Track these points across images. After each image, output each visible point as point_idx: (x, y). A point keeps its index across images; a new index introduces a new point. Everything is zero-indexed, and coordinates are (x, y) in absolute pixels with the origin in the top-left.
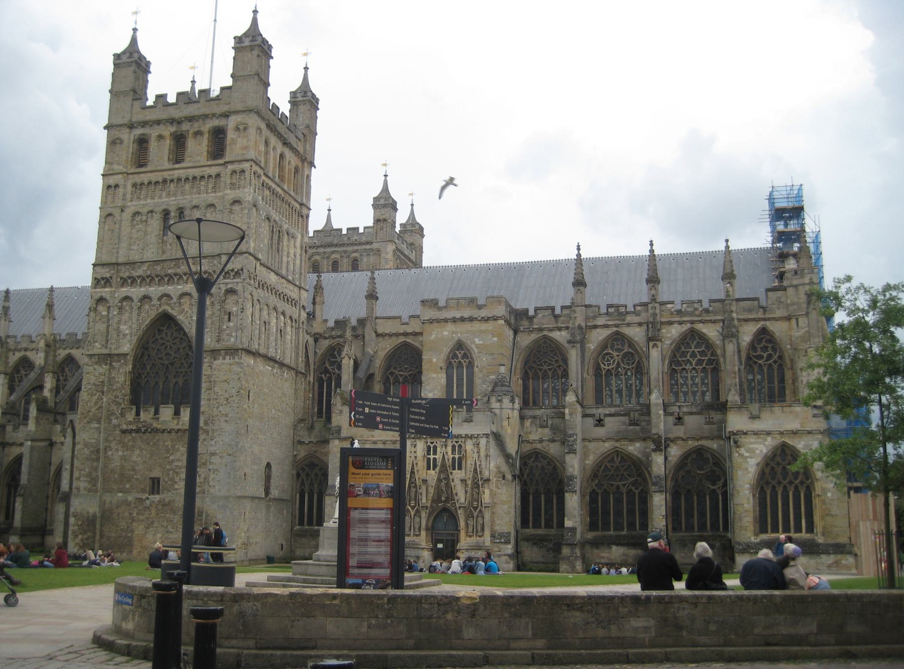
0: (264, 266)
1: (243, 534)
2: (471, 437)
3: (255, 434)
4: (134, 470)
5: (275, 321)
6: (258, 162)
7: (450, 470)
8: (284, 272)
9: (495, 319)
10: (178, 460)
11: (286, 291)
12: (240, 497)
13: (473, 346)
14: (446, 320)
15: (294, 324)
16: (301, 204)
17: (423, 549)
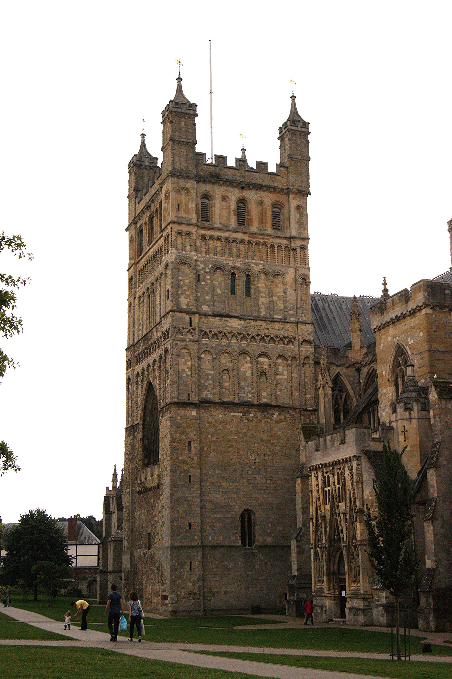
0: (215, 316)
1: (190, 584)
2: (347, 461)
3: (213, 483)
4: (142, 528)
5: (249, 365)
7: (336, 504)
8: (263, 313)
9: (419, 309)
10: (155, 516)
11: (263, 332)
12: (180, 547)
13: (407, 348)
14: (387, 324)
15: (289, 362)
16: (290, 238)
17: (326, 597)
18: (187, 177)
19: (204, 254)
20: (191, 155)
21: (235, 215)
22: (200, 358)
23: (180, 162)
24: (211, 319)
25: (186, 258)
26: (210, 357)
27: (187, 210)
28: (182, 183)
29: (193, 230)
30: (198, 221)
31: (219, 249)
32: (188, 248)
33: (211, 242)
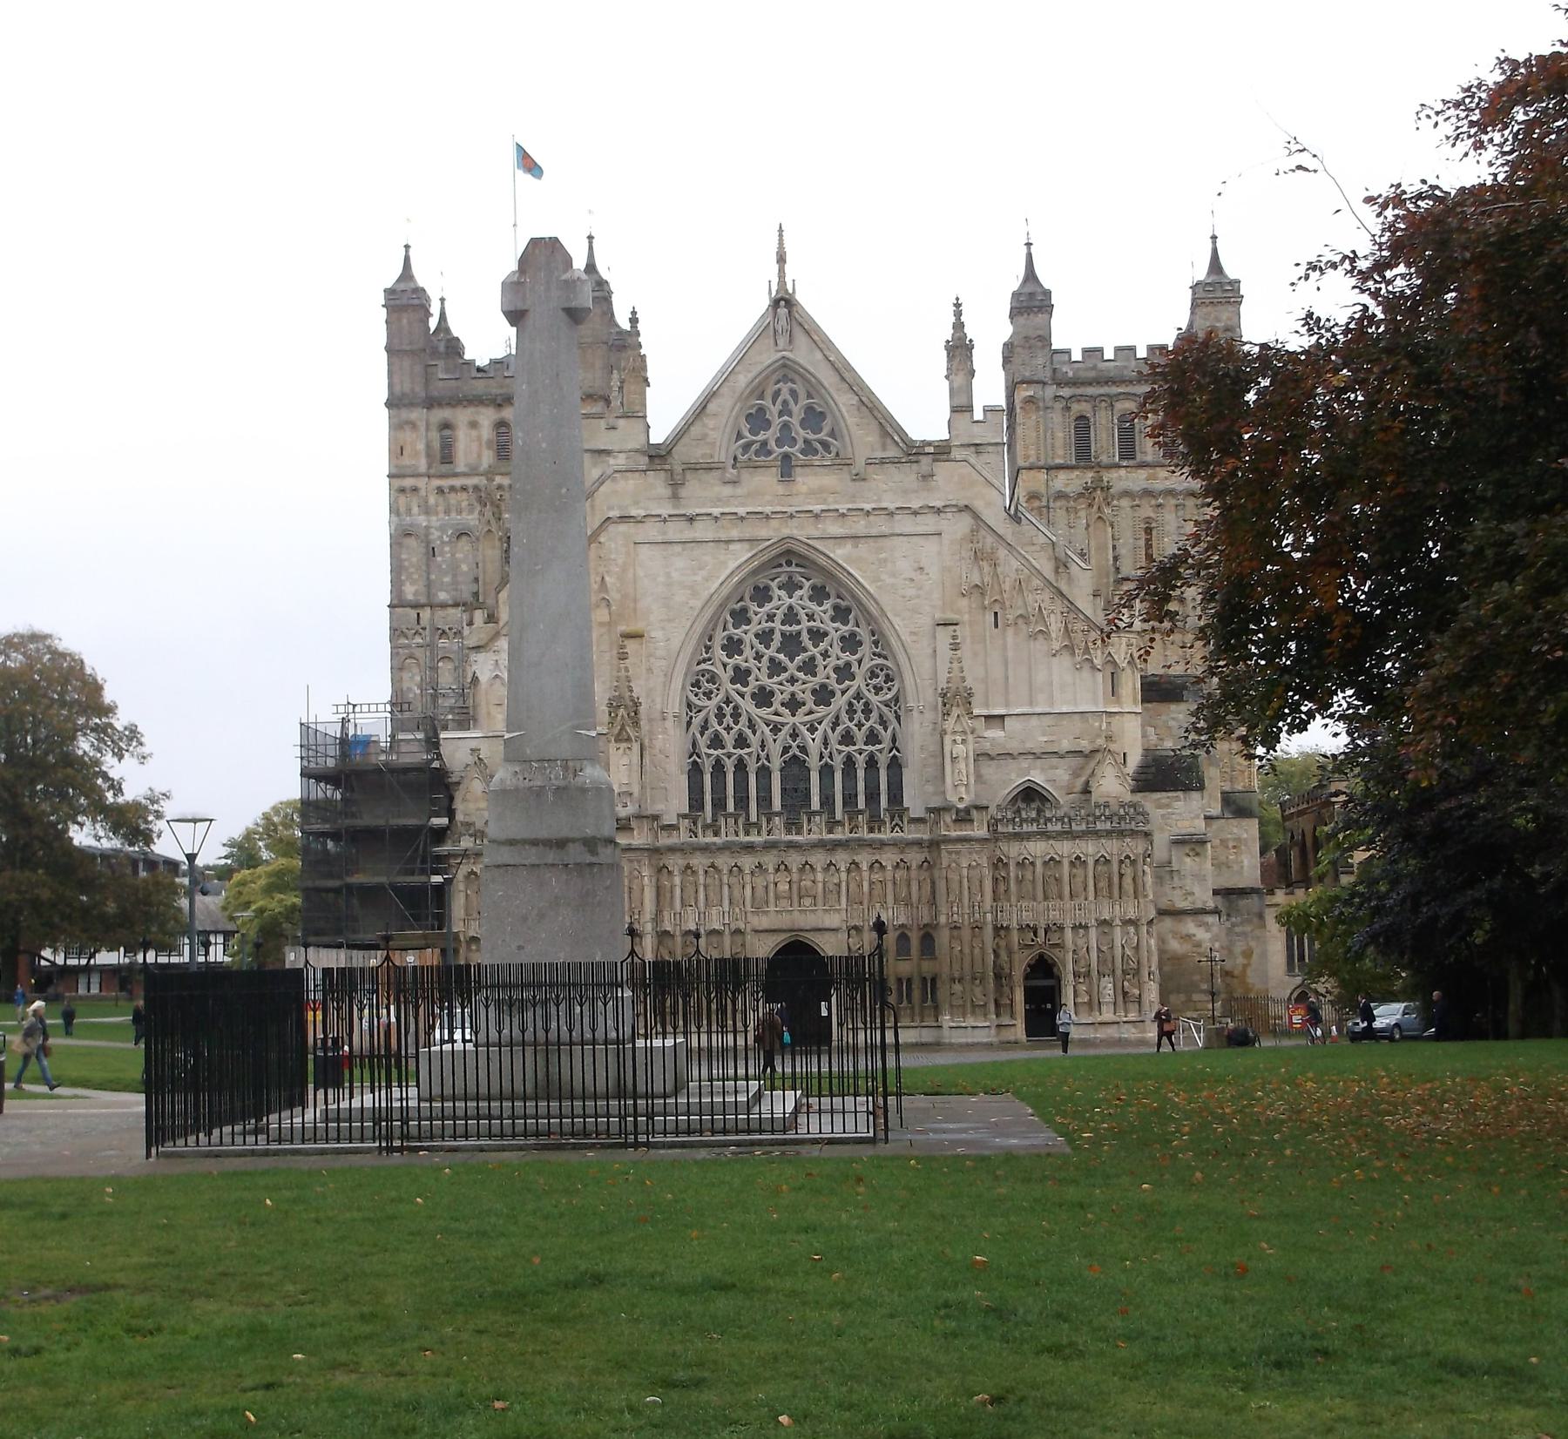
6: (408, 471)
18: (412, 405)
19: (441, 515)
20: (418, 369)
21: (489, 448)
22: (435, 669)
23: (402, 382)
24: (451, 611)
25: (411, 525)
26: (450, 666)
27: (416, 454)
28: (405, 414)
29: (421, 483)
30: (429, 467)
31: (464, 504)
32: (415, 510)
33: (453, 495)
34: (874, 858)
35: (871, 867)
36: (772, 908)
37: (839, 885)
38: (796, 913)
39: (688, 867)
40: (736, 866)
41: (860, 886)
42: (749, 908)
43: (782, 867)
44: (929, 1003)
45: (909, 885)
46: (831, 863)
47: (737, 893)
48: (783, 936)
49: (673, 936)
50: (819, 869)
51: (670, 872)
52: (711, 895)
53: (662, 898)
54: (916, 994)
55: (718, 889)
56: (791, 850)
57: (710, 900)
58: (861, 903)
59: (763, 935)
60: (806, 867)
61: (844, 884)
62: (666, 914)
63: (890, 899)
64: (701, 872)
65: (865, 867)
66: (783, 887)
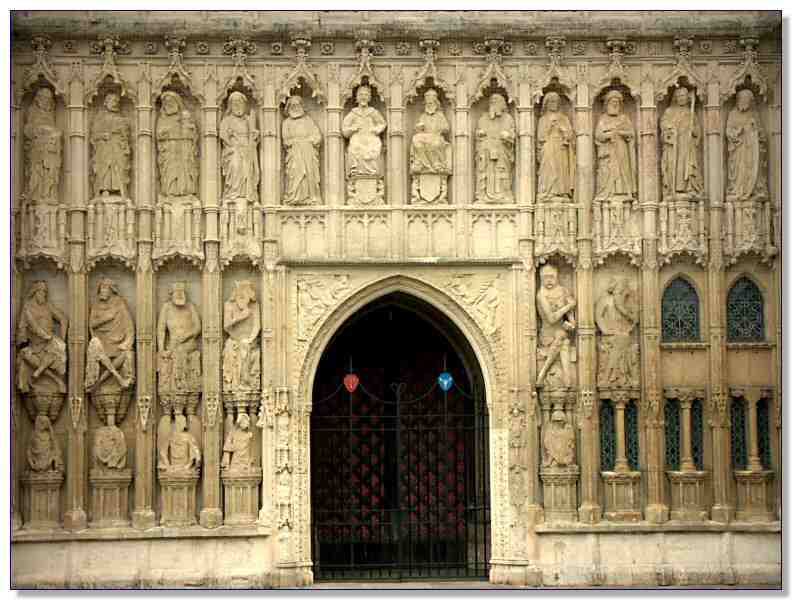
34: (616, 70)
35: (600, 101)
36: (334, 201)
37: (511, 145)
38: (396, 219)
39: (108, 87)
40: (239, 86)
41: (569, 146)
42: (270, 199)
43: (364, 93)
44: (754, 466)
45: (700, 148)
46: (493, 89)
47: (241, 163)
48: (373, 277)
49: (64, 273)
50: (462, 102)
51: (58, 101)
52: (171, 171)
53: (35, 168)
54: (717, 441)
55: (187, 148)
56: (391, 52)
57: (167, 180)
58: (571, 195)
59: (310, 275)
60: (428, 94)
61: (526, 144)
62: (43, 209)
63: (648, 183)
64: (145, 103)
65: (583, 98)
66: (366, 146)
